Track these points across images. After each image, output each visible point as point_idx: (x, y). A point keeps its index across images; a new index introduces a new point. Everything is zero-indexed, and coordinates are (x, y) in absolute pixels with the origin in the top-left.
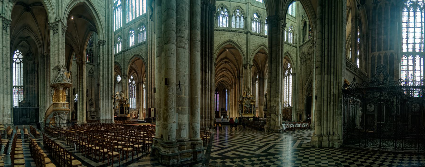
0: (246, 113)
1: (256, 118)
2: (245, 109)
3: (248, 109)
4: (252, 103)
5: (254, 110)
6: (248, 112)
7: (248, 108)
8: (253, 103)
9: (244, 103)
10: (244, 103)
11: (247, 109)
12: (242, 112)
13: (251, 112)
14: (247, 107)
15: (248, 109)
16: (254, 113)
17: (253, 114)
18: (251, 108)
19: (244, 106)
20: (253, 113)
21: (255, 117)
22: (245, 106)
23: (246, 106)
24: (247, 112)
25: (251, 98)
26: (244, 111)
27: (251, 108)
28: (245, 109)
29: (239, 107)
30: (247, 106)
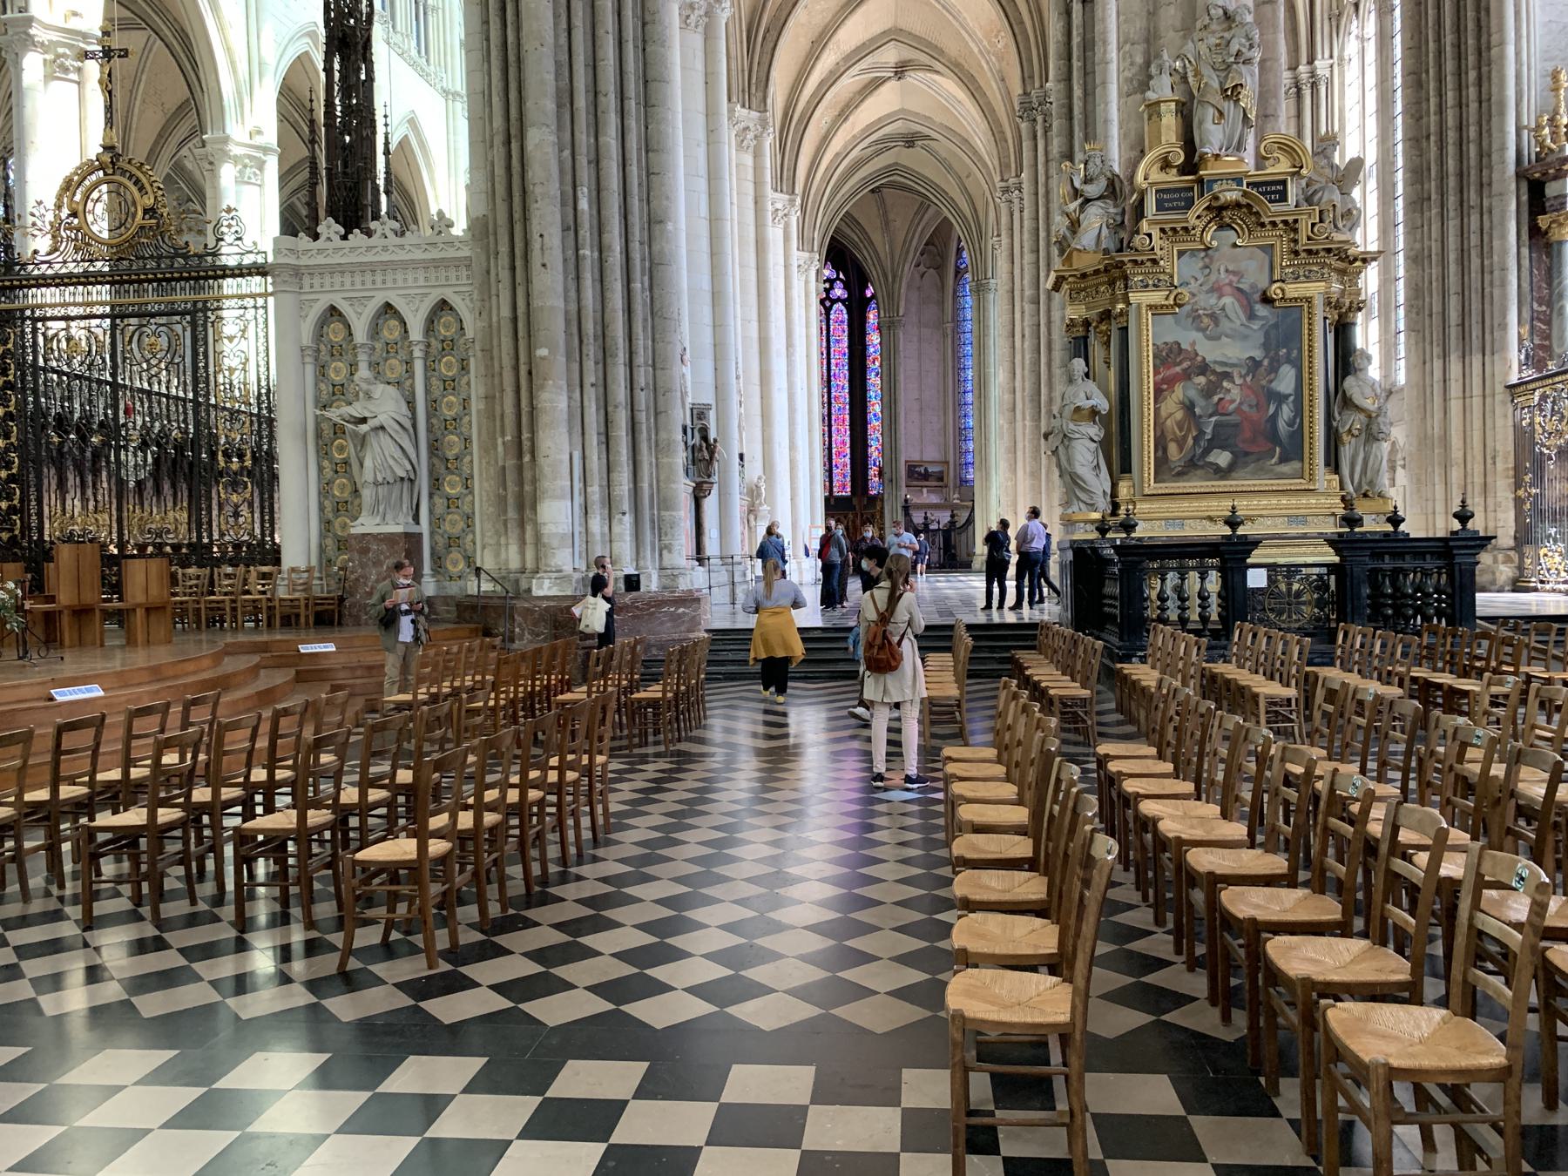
0: (1192, 465)
1: (1395, 545)
2: (1171, 405)
3: (1234, 393)
4: (1293, 290)
5: (1348, 403)
6: (1222, 458)
7: (1217, 377)
8: (1315, 289)
9: (1157, 297)
10: (1157, 297)
11: (1208, 393)
12: (1118, 455)
13: (1294, 449)
14: (1204, 369)
15: (1234, 393)
16: (1346, 453)
17: (1324, 478)
18: (1285, 381)
19: (1148, 337)
20: (1333, 463)
21: (1373, 525)
22: (1168, 355)
23: (1189, 338)
24: (1217, 442)
25: (1274, 187)
26: (1161, 444)
27: (1285, 381)
28: (1179, 392)
29: (1071, 381)
30: (1209, 351)
